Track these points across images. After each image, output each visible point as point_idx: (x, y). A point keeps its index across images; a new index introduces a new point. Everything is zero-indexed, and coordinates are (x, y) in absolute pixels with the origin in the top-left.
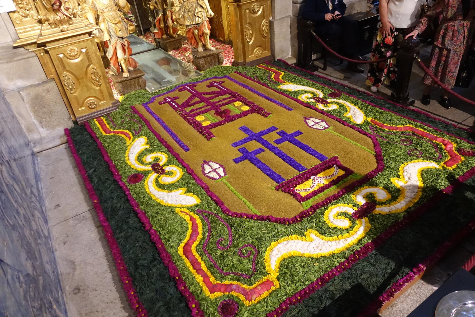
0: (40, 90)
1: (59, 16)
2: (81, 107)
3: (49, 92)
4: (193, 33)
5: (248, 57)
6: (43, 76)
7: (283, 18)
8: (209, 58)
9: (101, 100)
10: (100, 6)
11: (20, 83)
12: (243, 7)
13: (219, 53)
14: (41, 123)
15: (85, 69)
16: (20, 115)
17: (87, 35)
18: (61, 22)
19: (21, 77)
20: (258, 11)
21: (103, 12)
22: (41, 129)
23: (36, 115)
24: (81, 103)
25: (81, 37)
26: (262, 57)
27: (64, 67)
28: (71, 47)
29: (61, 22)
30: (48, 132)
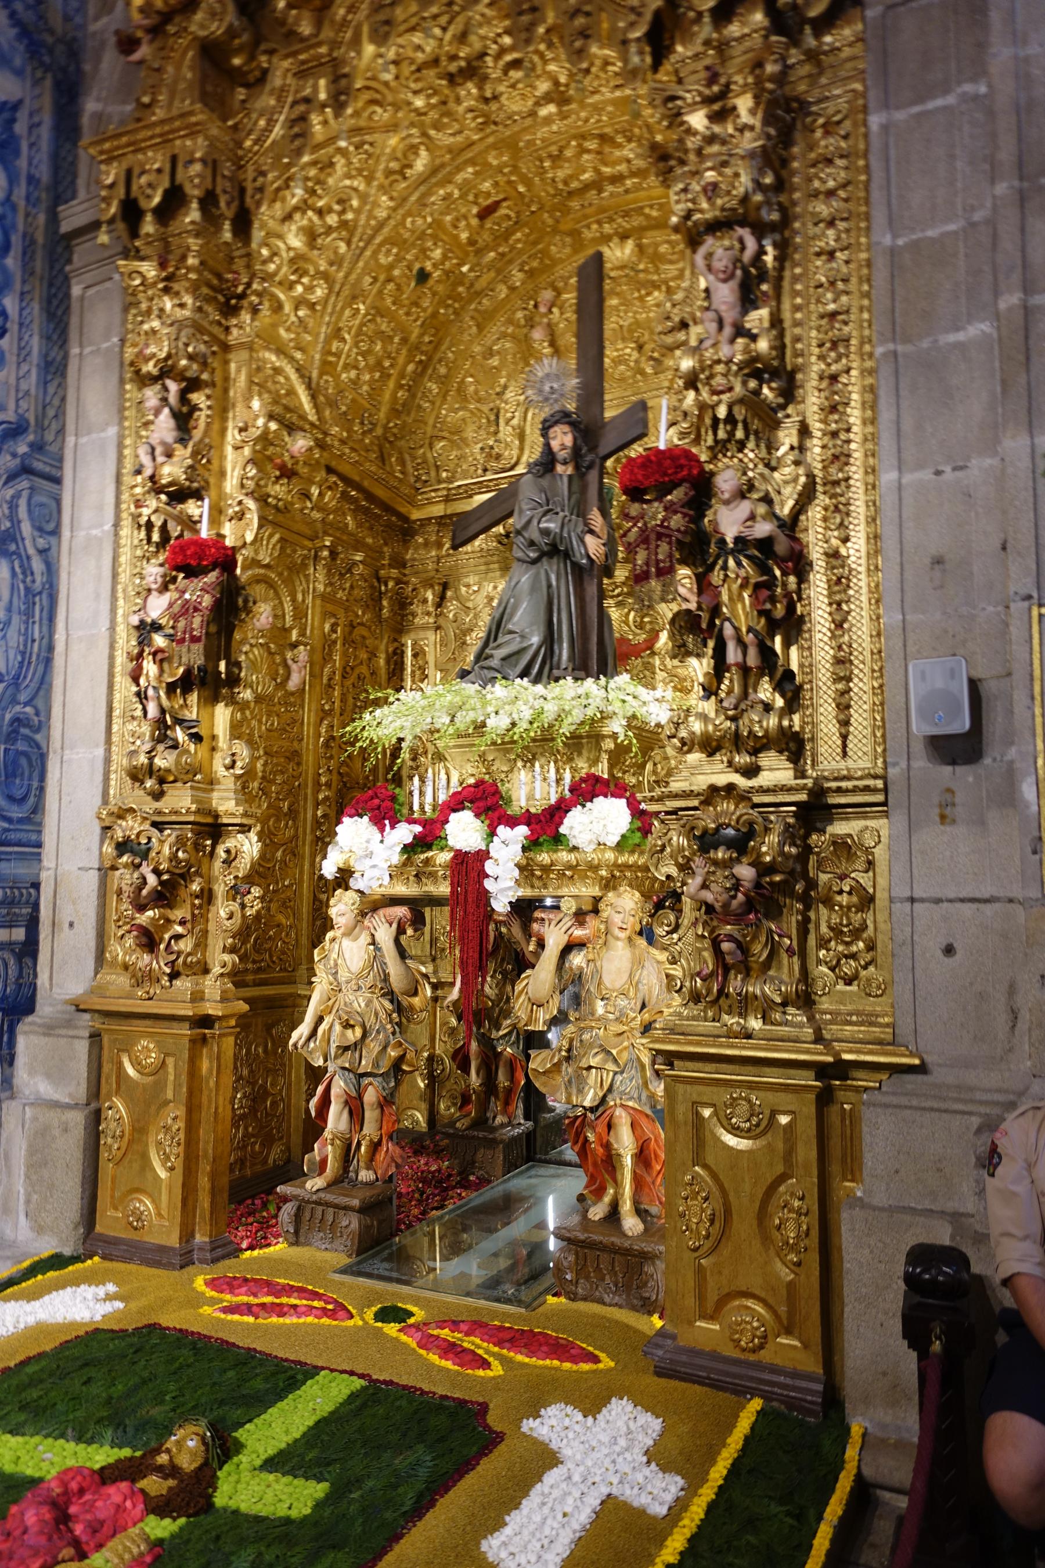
0: (54, 1117)
3: (66, 1130)
5: (691, 1323)
6: (81, 1092)
7: (913, 1211)
8: (605, 1257)
10: (343, 975)
11: (45, 1088)
13: (646, 1257)
14: (28, 1202)
17: (187, 1025)
19: (48, 1076)
20: (735, 1131)
22: (22, 1218)
23: (27, 1176)
25: (175, 1024)
30: (30, 1235)
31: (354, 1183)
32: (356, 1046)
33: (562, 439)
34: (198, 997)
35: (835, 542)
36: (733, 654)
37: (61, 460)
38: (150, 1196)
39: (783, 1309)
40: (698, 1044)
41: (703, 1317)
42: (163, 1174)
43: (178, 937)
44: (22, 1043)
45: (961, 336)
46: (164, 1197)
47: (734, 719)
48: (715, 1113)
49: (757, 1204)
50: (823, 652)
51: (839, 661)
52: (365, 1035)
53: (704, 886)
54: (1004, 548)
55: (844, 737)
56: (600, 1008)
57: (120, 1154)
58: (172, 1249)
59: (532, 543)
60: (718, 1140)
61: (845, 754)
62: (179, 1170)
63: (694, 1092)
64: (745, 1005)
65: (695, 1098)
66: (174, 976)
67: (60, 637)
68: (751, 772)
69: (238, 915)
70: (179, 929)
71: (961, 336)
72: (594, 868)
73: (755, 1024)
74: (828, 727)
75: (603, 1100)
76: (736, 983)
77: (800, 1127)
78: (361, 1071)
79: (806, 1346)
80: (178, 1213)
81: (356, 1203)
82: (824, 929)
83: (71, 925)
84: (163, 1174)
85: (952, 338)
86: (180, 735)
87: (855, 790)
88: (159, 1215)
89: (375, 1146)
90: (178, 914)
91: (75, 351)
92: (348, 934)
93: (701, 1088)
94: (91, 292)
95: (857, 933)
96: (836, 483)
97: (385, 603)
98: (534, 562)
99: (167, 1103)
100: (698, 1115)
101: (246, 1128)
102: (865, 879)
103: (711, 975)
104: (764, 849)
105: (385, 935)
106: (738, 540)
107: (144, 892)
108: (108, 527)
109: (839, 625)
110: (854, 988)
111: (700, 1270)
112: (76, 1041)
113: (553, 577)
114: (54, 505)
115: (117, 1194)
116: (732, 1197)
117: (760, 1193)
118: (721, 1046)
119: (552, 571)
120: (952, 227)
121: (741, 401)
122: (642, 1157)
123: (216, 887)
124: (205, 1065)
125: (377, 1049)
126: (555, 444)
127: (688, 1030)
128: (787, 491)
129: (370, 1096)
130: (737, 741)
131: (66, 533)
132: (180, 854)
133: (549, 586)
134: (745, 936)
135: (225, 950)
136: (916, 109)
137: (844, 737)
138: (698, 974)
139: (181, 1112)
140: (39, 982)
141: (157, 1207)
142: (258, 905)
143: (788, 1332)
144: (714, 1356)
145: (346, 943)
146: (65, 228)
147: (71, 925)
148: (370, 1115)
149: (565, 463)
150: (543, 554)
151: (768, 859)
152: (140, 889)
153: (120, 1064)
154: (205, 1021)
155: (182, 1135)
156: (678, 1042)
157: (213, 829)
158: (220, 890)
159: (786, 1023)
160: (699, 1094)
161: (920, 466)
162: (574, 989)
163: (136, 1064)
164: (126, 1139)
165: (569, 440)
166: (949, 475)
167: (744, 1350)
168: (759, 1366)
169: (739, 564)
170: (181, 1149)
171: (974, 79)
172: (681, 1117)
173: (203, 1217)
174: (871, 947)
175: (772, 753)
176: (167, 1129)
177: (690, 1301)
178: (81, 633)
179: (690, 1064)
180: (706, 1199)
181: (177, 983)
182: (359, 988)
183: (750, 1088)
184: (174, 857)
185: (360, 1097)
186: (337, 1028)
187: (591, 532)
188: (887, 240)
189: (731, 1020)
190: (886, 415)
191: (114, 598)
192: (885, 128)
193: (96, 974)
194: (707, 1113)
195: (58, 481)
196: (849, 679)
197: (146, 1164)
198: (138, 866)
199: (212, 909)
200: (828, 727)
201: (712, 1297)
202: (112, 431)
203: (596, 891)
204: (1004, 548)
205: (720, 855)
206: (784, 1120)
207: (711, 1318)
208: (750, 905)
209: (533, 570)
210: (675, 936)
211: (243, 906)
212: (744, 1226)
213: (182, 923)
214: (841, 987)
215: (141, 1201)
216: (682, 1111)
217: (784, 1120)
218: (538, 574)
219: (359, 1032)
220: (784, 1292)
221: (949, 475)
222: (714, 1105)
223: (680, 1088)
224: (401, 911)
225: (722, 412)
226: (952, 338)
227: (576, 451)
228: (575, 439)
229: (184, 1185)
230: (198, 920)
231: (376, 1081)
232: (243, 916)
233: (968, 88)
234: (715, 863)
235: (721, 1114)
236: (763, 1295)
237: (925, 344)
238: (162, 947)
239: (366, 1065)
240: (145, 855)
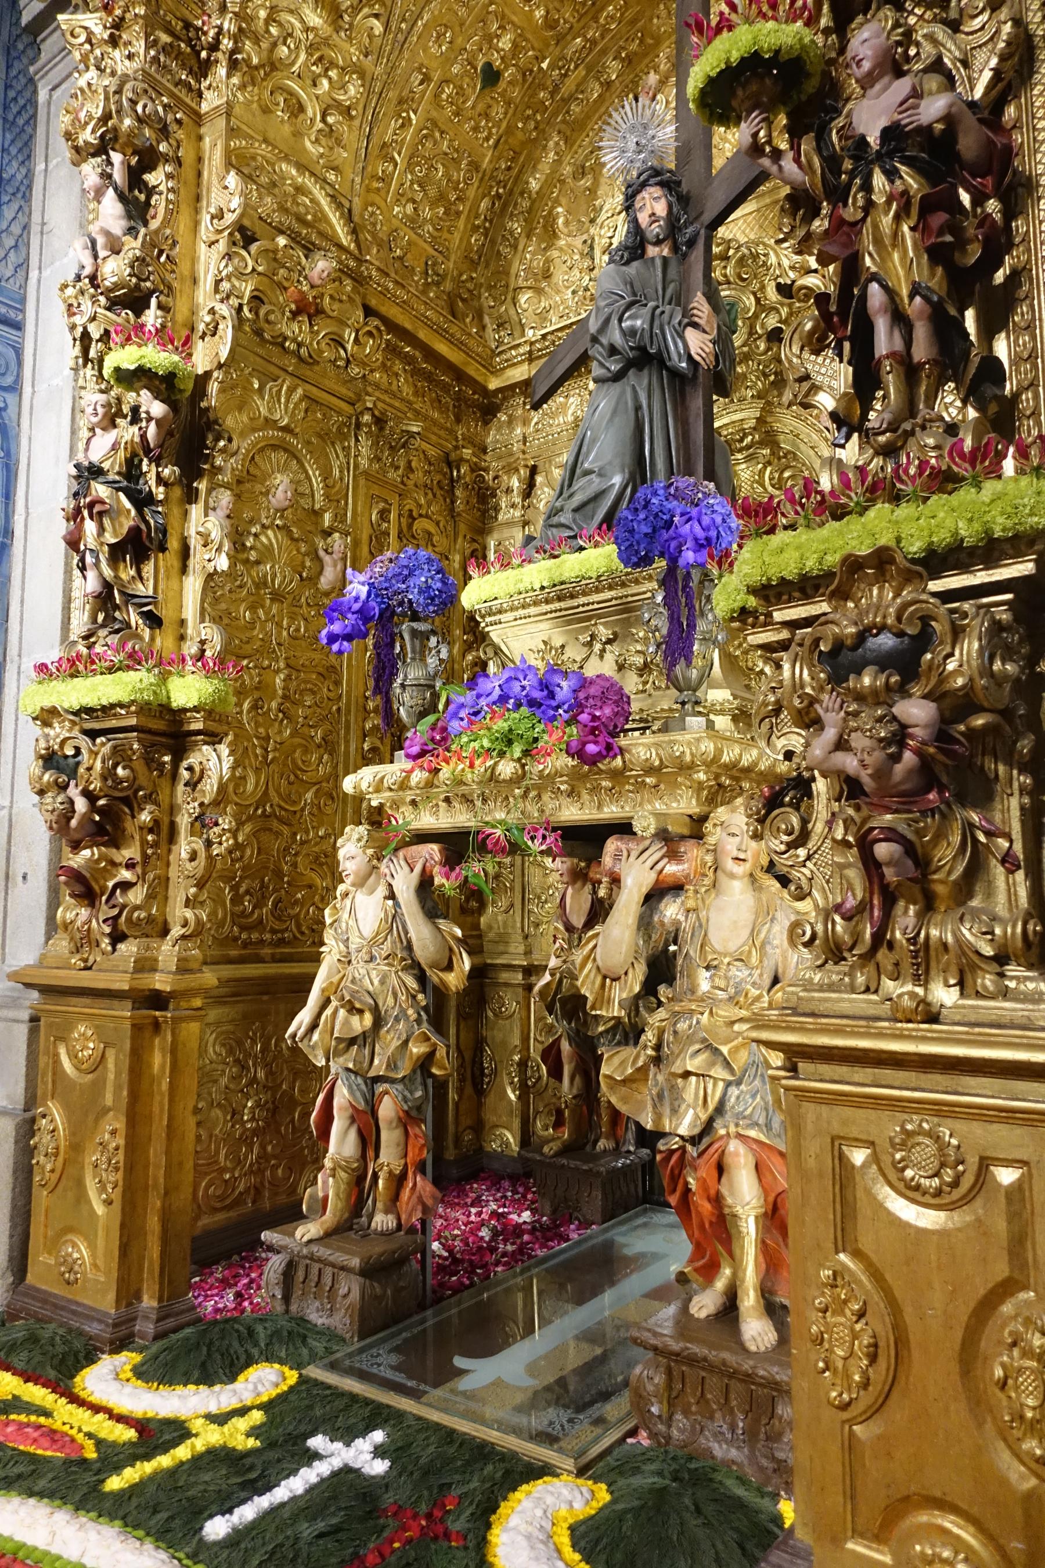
10: (355, 942)
17: (129, 1004)
20: (912, 1192)
31: (366, 1233)
32: (366, 1039)
34: (145, 965)
37: (23, 300)
38: (86, 1238)
40: (839, 1031)
41: (858, 1533)
42: (100, 1209)
46: (101, 1243)
47: (889, 451)
48: (875, 1158)
49: (958, 1334)
52: (378, 1022)
53: (841, 745)
56: (704, 982)
57: (55, 1177)
58: (106, 1314)
59: (613, 351)
60: (880, 1206)
62: (117, 1206)
63: (836, 1118)
64: (923, 962)
65: (837, 1129)
66: (117, 937)
69: (202, 854)
70: (126, 875)
73: (944, 994)
78: (372, 1074)
80: (115, 1265)
81: (355, 1262)
83: (24, 878)
84: (100, 1209)
88: (95, 1265)
89: (399, 1181)
93: (848, 1112)
97: (458, 493)
98: (617, 377)
99: (106, 1111)
101: (263, 1147)
103: (863, 908)
104: (951, 666)
105: (405, 883)
106: (890, 133)
107: (74, 823)
111: (851, 1444)
112: (16, 1026)
114: (12, 354)
116: (909, 1315)
117: (963, 1312)
118: (881, 1035)
119: (640, 382)
122: (774, 1217)
123: (178, 819)
124: (158, 1060)
125: (396, 1043)
126: (643, 218)
127: (822, 1008)
129: (387, 1109)
131: (27, 389)
132: (120, 771)
133: (638, 408)
134: (920, 833)
135: (188, 903)
138: (837, 908)
139: (120, 1124)
141: (93, 1256)
142: (228, 842)
147: (24, 878)
148: (389, 1137)
149: (658, 242)
150: (630, 365)
151: (960, 681)
152: (69, 819)
153: (57, 1055)
154: (157, 1000)
155: (121, 1156)
156: (801, 1029)
158: (183, 821)
159: (1005, 994)
160: (845, 1123)
163: (73, 1056)
164: (61, 1159)
165: (661, 208)
170: (120, 1175)
172: (811, 1163)
173: (151, 1271)
179: (825, 1069)
180: (861, 1315)
181: (121, 947)
182: (372, 959)
183: (938, 1114)
184: (108, 774)
187: (695, 325)
193: (48, 938)
194: (858, 1156)
195: (18, 326)
197: (81, 1196)
198: (64, 787)
203: (695, 809)
205: (867, 681)
206: (1006, 1176)
207: (879, 1537)
209: (616, 388)
210: (802, 852)
211: (209, 844)
212: (933, 1371)
213: (130, 866)
215: (74, 1245)
216: (815, 1150)
217: (1006, 1176)
218: (623, 393)
219: (368, 1019)
220: (1018, 1513)
222: (871, 1144)
223: (810, 1111)
228: (670, 206)
229: (123, 1226)
231: (395, 1089)
232: (210, 858)
234: (860, 697)
235: (886, 1160)
236: (975, 1511)
239: (379, 1066)
240: (73, 774)
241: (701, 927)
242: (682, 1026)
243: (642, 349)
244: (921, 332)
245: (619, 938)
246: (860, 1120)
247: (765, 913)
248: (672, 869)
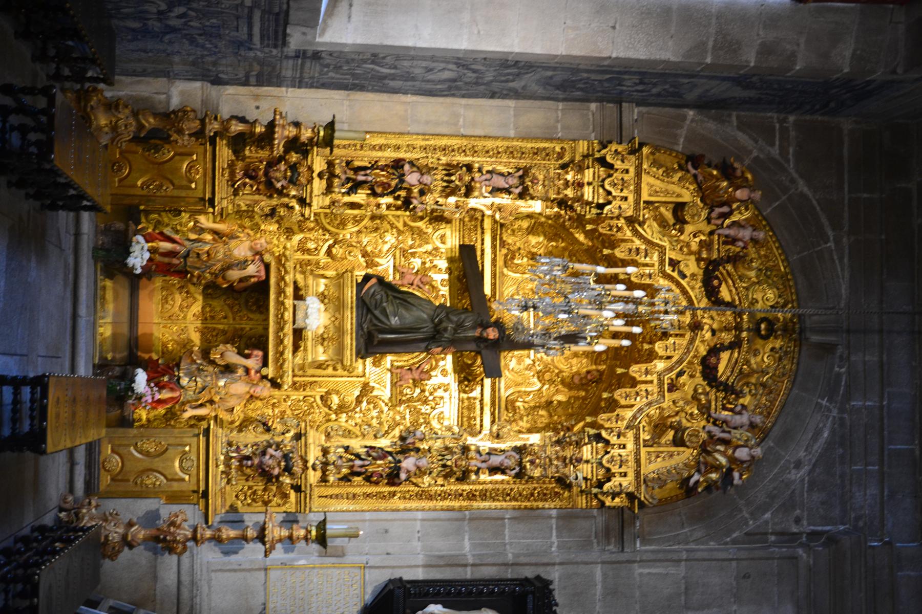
1: (239, 174)
2: (121, 153)
4: (164, 375)
9: (120, 181)
10: (233, 243)
12: (195, 439)
15: (170, 177)
16: (139, 82)
18: (232, 174)
21: (225, 243)
24: (126, 155)
26: (102, 471)
27: (181, 154)
28: (201, 170)
29: (232, 174)
33: (492, 334)
35: (399, 495)
36: (358, 462)
39: (119, 477)
42: (139, 183)
43: (252, 186)
44: (198, 84)
45: (466, 540)
47: (333, 463)
50: (358, 490)
51: (354, 496)
54: (388, 554)
55: (326, 497)
59: (441, 322)
61: (320, 497)
64: (228, 465)
67: (410, 98)
68: (314, 469)
71: (466, 540)
72: (281, 377)
73: (222, 468)
74: (330, 491)
75: (183, 388)
76: (235, 463)
77: (184, 484)
79: (108, 486)
82: (255, 488)
83: (258, 108)
85: (467, 537)
86: (349, 185)
87: (305, 503)
90: (261, 187)
91: (561, 105)
92: (251, 248)
94: (590, 113)
95: (254, 500)
96: (421, 495)
98: (433, 321)
100: (186, 445)
102: (273, 503)
105: (251, 269)
108: (462, 131)
109: (368, 496)
110: (234, 498)
111: (129, 446)
113: (425, 330)
115: (126, 155)
116: (157, 459)
117: (160, 469)
119: (428, 327)
120: (507, 538)
121: (452, 470)
125: (198, 266)
128: (420, 480)
129: (175, 261)
130: (325, 464)
136: (554, 526)
137: (326, 497)
140: (228, 87)
143: (112, 479)
144: (100, 453)
145: (247, 244)
146: (624, 104)
147: (258, 108)
148: (166, 260)
149: (481, 334)
150: (436, 326)
157: (302, 202)
161: (422, 526)
162: (228, 369)
163: (190, 168)
165: (491, 337)
166: (417, 535)
167: (103, 463)
168: (99, 469)
169: (390, 468)
171: (558, 547)
174: (249, 505)
175: (321, 475)
176: (161, 186)
177: (117, 442)
178: (409, 111)
185: (175, 257)
186: (207, 248)
188: (508, 516)
189: (222, 458)
190: (443, 515)
191: (424, 135)
192: (550, 517)
194: (187, 448)
196: (347, 498)
198: (285, 178)
199: (265, 198)
200: (330, 491)
201: (122, 450)
202: (512, 133)
204: (388, 554)
206: (187, 477)
207: (113, 451)
208: (264, 470)
212: (147, 463)
213: (257, 189)
214: (234, 494)
221: (417, 535)
224: (263, 273)
225: (449, 463)
226: (467, 537)
227: (486, 340)
230: (258, 191)
233: (556, 544)
234: (280, 462)
237: (467, 528)
238: (247, 180)
239: (190, 260)
241: (236, 381)
242: (209, 378)
243: (438, 332)
244: (359, 470)
245: (233, 357)
246: (194, 450)
247: (240, 397)
248: (253, 372)
